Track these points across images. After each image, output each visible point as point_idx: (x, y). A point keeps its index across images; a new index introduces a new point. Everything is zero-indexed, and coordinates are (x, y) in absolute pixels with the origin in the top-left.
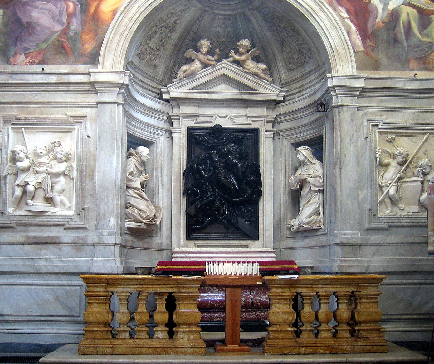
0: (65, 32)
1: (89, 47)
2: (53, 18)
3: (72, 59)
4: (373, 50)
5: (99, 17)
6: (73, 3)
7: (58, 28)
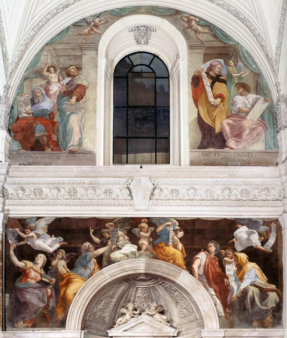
0: (46, 307)
1: (60, 317)
2: (39, 299)
3: (51, 324)
4: (230, 315)
5: (66, 298)
6: (51, 289)
7: (42, 305)
